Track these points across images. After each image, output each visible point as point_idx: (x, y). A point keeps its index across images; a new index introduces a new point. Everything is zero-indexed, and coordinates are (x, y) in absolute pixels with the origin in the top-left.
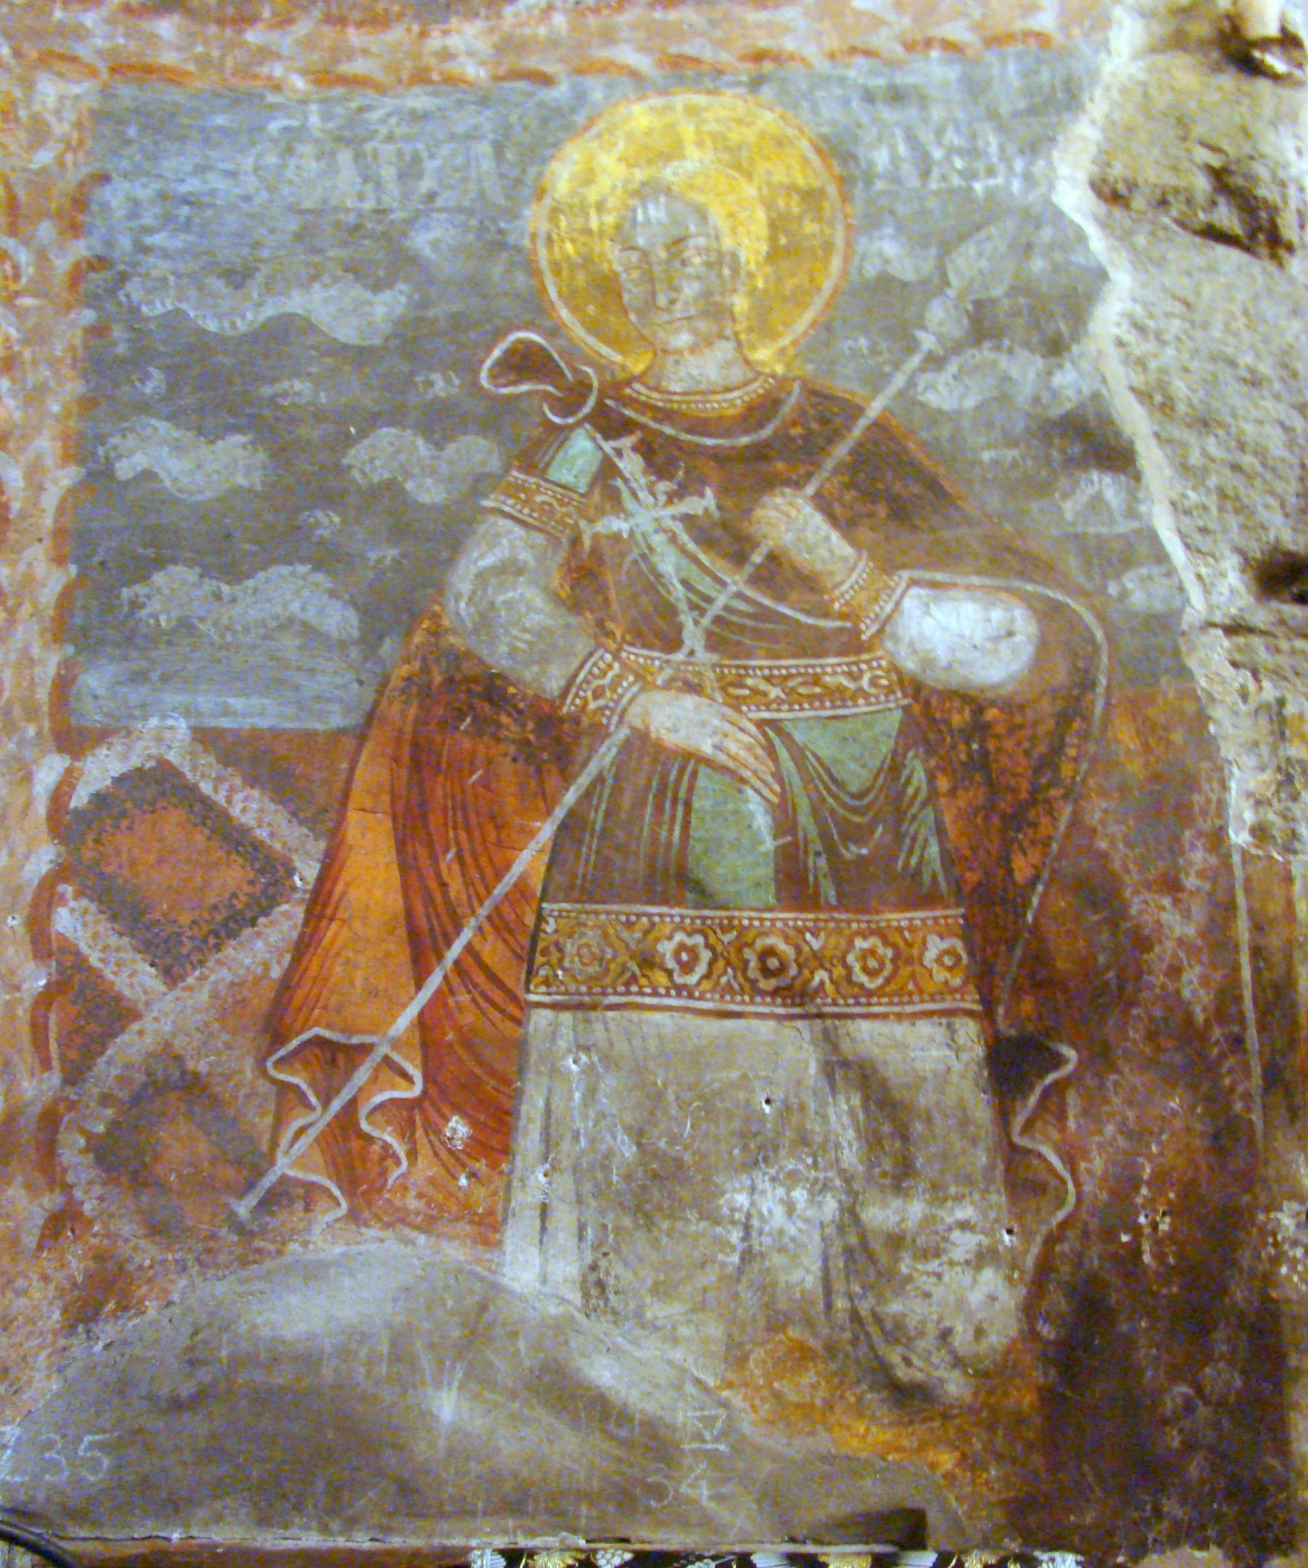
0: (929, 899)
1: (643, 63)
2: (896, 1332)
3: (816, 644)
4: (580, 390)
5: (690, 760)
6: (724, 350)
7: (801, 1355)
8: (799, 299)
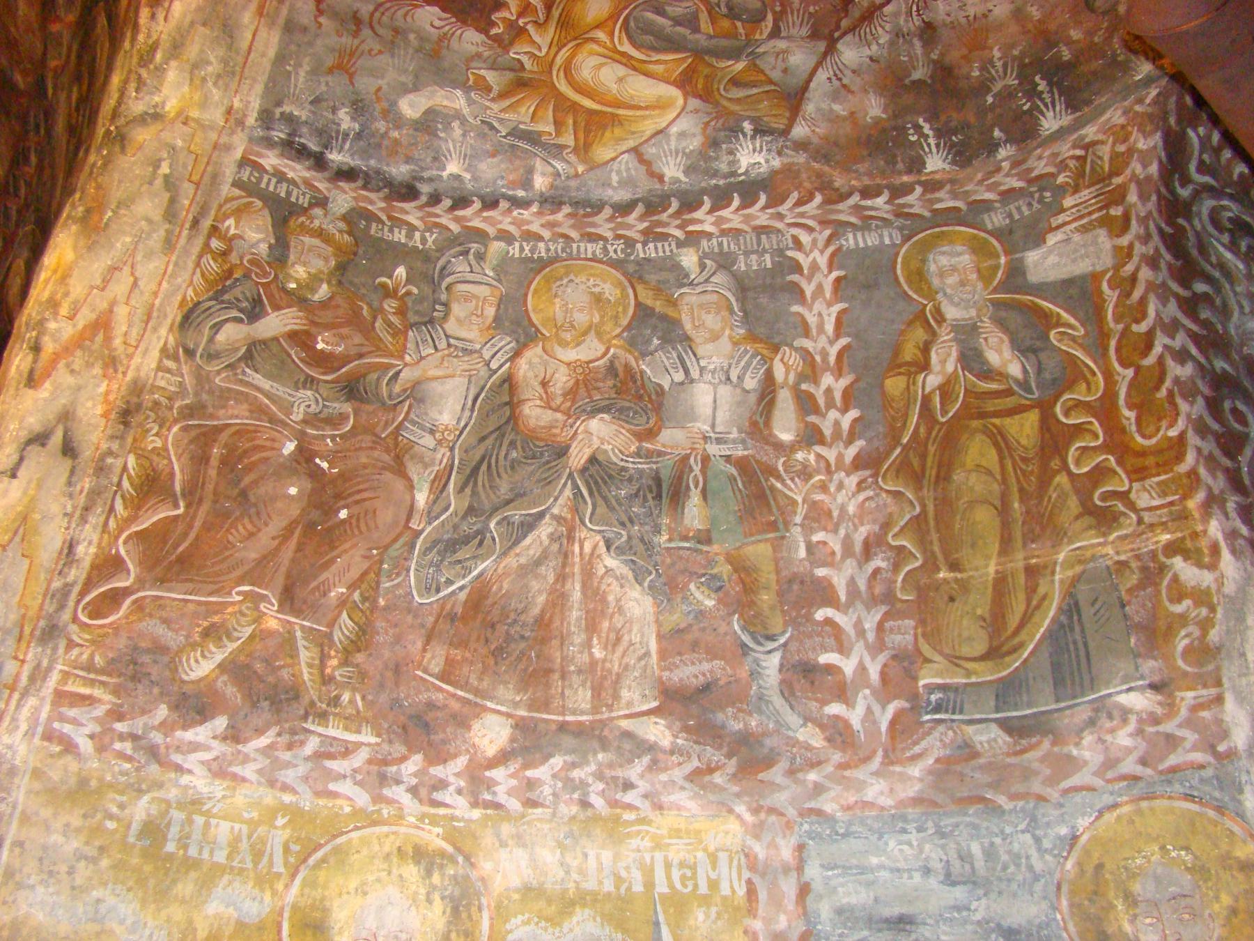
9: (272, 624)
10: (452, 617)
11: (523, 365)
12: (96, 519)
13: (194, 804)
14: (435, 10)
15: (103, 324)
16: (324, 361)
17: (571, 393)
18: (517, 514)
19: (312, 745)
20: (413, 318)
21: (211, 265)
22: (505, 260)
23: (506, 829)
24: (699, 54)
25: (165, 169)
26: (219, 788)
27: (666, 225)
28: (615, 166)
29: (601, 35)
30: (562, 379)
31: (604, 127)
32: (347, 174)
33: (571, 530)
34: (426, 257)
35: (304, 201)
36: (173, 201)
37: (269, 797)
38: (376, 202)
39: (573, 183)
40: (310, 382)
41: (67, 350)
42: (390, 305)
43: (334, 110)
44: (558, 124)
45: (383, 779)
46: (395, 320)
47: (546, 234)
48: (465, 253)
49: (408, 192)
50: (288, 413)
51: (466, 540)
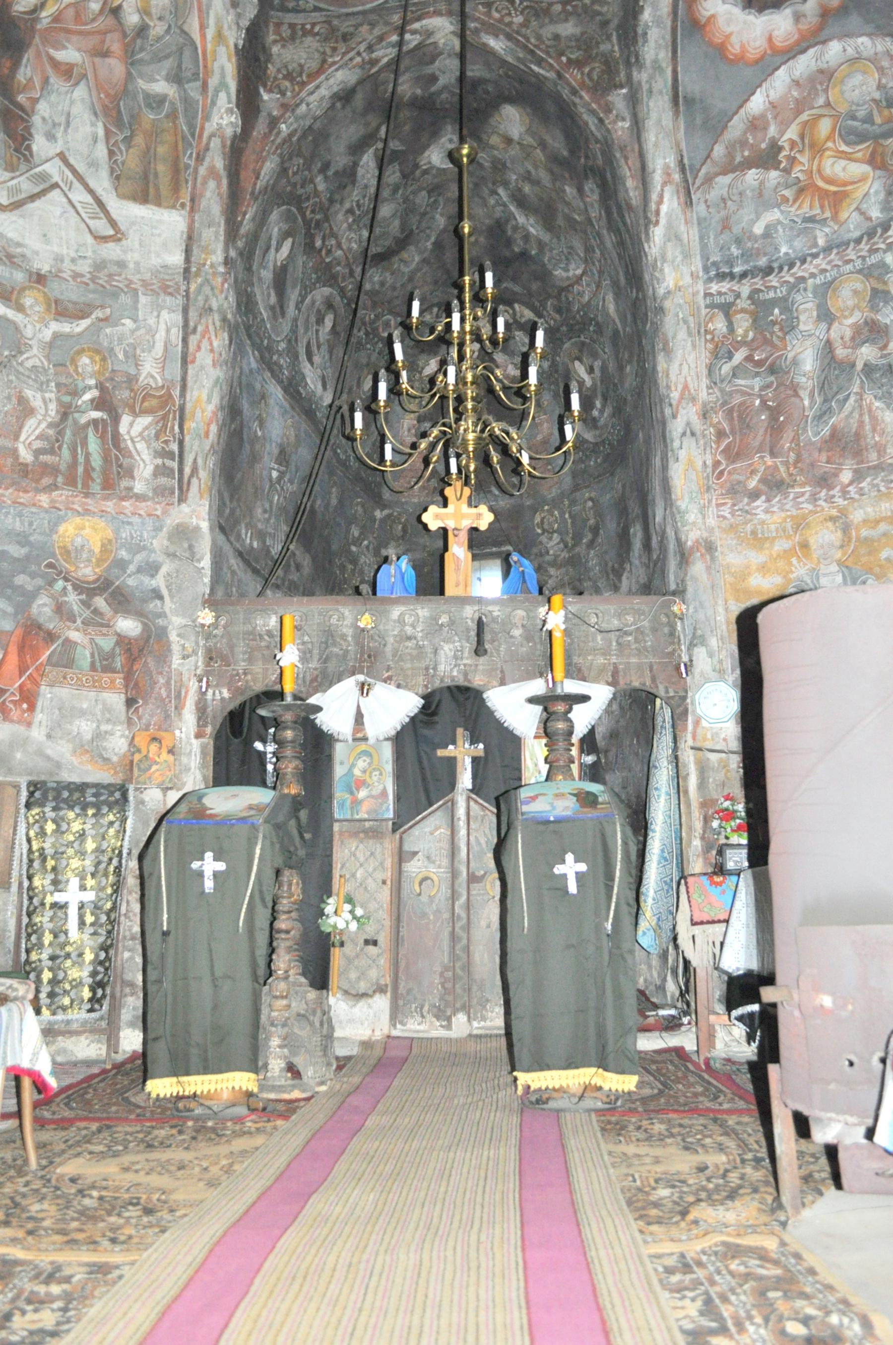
0: (118, 672)
1: (80, 509)
2: (105, 749)
3: (102, 625)
4: (61, 572)
5: (76, 643)
6: (90, 569)
7: (87, 751)
8: (105, 560)
9: (770, 463)
10: (826, 442)
11: (832, 332)
12: (708, 451)
13: (763, 522)
14: (753, 171)
15: (686, 387)
16: (759, 364)
17: (853, 339)
18: (840, 397)
19: (792, 496)
20: (787, 330)
21: (710, 346)
22: (816, 286)
23: (856, 504)
24: (876, 138)
25: (681, 316)
26: (768, 516)
27: (877, 243)
28: (850, 220)
29: (830, 144)
30: (848, 333)
31: (841, 201)
32: (744, 275)
33: (861, 396)
34: (785, 299)
35: (732, 300)
36: (688, 328)
37: (783, 515)
38: (758, 282)
39: (835, 236)
40: (757, 374)
41: (679, 402)
42: (776, 328)
43: (729, 249)
44: (822, 207)
45: (816, 500)
46: (780, 334)
47: (829, 268)
48: (798, 291)
49: (768, 271)
50: (752, 388)
51: (825, 413)
